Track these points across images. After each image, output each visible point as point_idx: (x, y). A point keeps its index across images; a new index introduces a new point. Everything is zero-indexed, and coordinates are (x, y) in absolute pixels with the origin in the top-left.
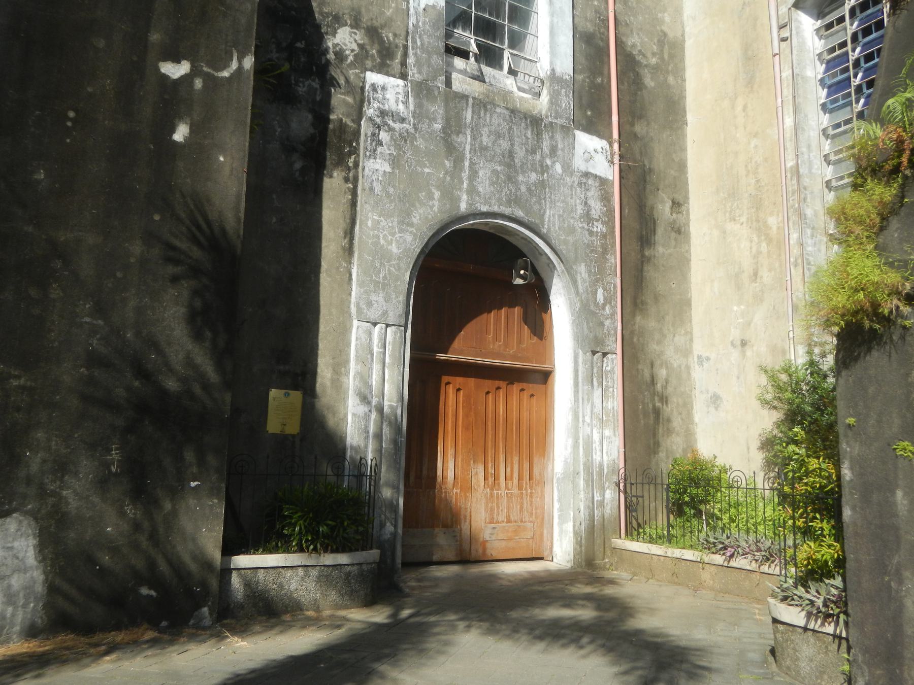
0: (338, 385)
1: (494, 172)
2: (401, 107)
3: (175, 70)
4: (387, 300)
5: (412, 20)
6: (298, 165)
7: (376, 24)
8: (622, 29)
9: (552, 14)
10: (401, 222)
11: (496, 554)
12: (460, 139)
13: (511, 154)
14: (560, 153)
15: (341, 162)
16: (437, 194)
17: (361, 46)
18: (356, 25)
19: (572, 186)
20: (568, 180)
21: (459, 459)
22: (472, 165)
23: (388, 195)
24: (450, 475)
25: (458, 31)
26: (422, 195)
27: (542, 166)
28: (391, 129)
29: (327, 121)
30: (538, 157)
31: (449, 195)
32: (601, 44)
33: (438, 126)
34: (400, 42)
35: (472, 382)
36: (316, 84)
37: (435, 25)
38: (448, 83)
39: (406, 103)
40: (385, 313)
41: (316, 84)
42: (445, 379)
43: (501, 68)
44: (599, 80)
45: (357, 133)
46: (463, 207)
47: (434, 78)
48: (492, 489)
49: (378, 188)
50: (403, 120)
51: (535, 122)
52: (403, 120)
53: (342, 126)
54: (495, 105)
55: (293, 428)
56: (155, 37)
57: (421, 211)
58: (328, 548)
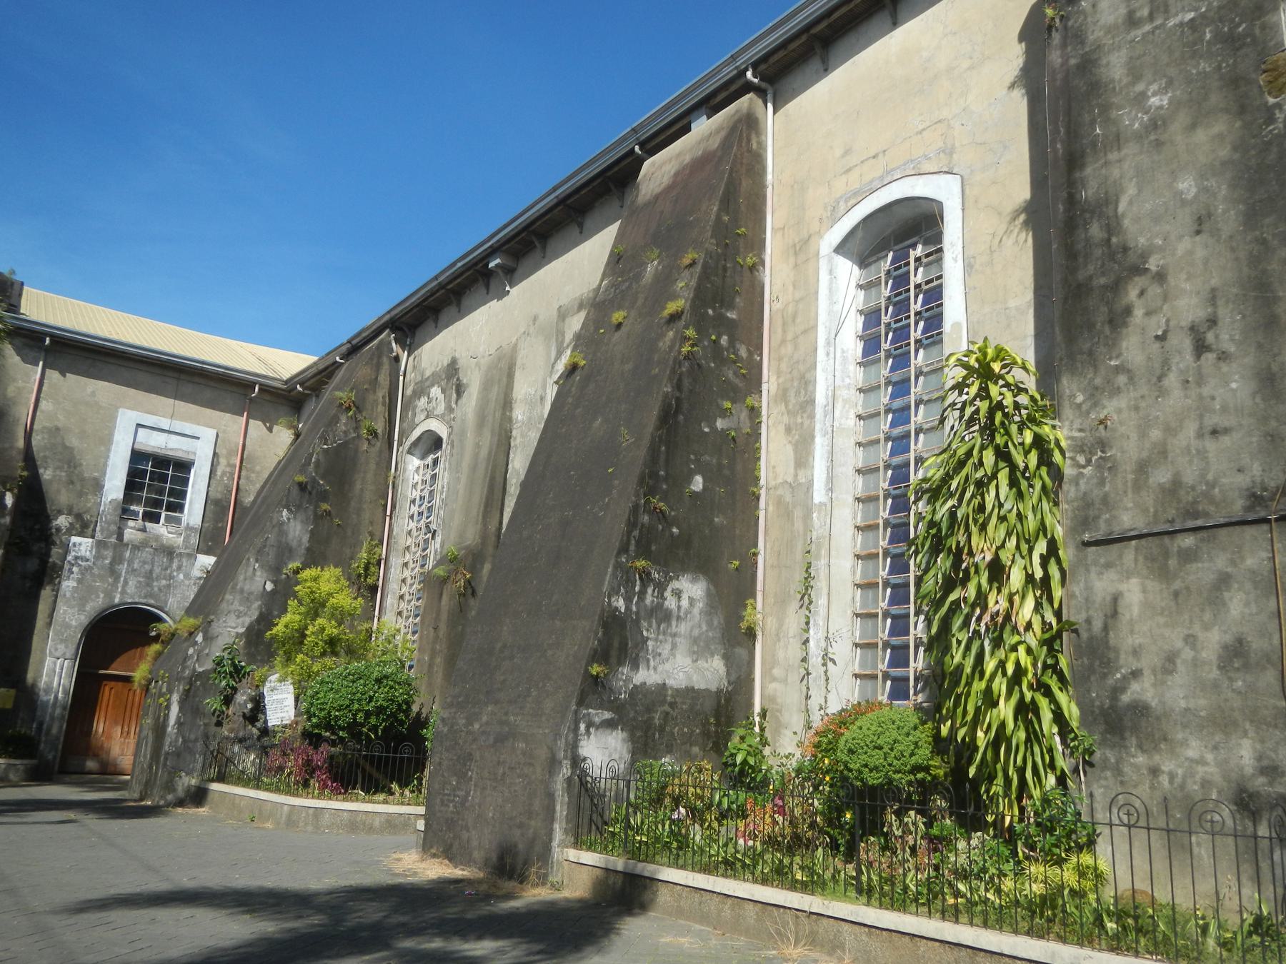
1: (139, 582)
4: (66, 647)
5: (102, 508)
6: (28, 585)
8: (241, 494)
9: (192, 493)
12: (121, 566)
13: (151, 571)
15: (51, 581)
16: (102, 595)
18: (69, 514)
20: (187, 582)
21: (107, 723)
24: (101, 730)
26: (93, 596)
28: (80, 565)
29: (48, 562)
31: (109, 594)
32: (225, 504)
33: (107, 562)
34: (94, 519)
35: (120, 684)
36: (43, 545)
37: (115, 510)
38: (120, 536)
39: (91, 551)
40: (64, 654)
42: (105, 683)
43: (158, 522)
45: (62, 568)
46: (117, 601)
47: (110, 537)
49: (68, 594)
50: (87, 560)
51: (169, 552)
52: (87, 560)
53: (54, 564)
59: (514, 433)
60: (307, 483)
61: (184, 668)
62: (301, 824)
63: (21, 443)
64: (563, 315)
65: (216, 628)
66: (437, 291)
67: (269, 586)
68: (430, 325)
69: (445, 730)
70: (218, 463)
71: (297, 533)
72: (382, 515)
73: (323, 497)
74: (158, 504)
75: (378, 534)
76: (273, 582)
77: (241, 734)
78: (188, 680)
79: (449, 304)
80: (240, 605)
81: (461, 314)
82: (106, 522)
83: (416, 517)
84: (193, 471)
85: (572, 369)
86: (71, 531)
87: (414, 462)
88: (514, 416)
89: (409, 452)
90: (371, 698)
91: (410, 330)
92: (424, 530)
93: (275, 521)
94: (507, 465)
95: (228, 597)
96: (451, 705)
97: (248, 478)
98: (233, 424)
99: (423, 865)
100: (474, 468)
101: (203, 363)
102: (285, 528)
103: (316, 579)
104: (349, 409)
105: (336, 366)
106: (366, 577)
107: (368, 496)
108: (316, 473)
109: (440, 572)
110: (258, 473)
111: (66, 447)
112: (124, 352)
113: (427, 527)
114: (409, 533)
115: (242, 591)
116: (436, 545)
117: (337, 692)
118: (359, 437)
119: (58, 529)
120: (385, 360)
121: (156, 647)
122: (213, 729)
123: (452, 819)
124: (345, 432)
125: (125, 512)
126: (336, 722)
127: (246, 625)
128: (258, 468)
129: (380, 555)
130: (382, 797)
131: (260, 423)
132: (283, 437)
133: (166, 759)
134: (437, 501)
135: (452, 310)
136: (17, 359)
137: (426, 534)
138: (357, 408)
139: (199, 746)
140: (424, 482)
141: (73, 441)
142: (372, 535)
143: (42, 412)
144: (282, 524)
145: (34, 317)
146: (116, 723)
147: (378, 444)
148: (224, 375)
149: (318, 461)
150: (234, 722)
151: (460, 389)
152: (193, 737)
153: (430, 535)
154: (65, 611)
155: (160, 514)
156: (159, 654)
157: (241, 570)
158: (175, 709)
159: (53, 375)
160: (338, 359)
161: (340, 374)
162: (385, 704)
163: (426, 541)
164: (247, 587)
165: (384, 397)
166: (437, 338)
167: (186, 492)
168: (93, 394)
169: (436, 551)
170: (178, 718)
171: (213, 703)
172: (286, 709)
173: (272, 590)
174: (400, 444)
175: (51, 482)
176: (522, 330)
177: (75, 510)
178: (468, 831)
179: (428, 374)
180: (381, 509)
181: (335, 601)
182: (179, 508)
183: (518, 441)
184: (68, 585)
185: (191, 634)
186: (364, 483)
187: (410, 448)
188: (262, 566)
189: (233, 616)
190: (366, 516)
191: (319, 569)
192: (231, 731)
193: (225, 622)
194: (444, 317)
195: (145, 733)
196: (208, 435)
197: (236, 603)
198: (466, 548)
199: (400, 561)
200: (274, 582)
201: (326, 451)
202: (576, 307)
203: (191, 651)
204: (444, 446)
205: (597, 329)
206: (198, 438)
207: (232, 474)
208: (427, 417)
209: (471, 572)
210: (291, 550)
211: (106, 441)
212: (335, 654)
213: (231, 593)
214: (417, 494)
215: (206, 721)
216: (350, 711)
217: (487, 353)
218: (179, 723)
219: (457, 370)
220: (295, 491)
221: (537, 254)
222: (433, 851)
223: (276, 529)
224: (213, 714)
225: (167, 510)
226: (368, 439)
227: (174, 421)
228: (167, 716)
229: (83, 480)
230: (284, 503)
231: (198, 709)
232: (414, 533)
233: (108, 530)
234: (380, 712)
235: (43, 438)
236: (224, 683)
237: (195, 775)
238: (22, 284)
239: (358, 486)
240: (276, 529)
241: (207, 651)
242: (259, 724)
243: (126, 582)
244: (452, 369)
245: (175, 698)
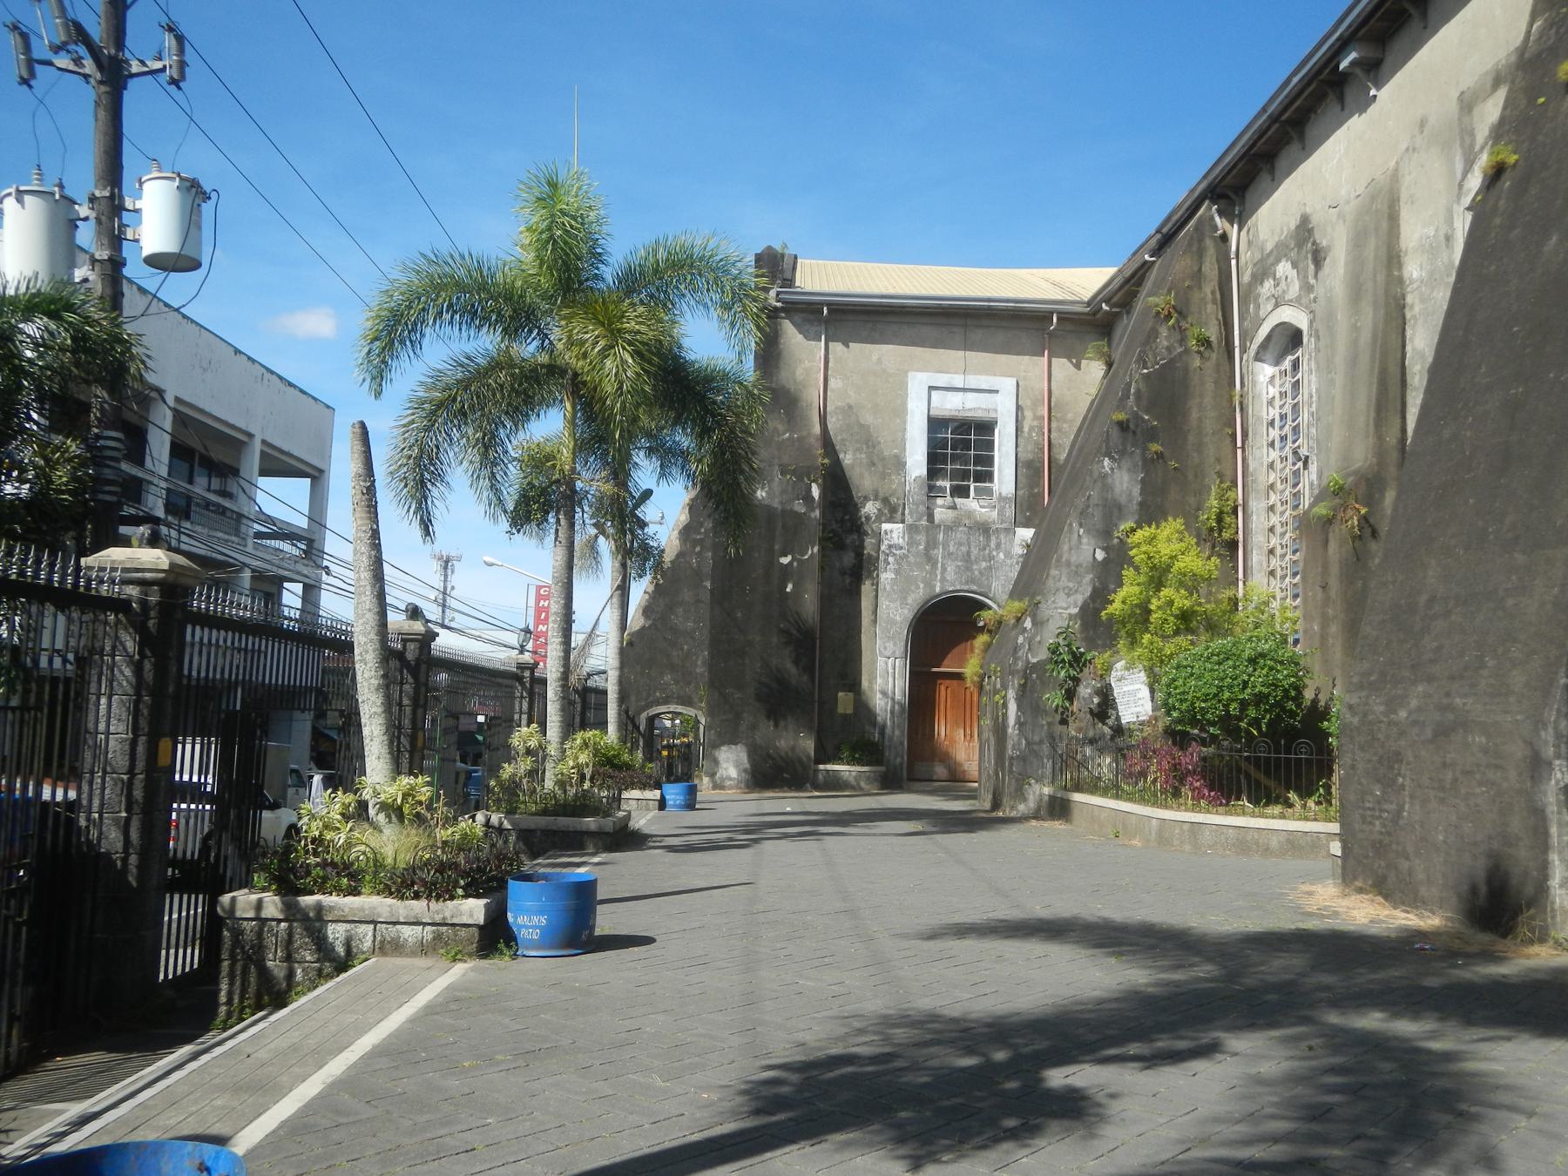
0: (871, 688)
1: (958, 567)
2: (901, 540)
3: (785, 560)
4: (895, 645)
5: (907, 488)
6: (848, 581)
7: (887, 495)
8: (1054, 450)
9: (1000, 458)
10: (902, 604)
11: (971, 779)
12: (936, 551)
13: (968, 553)
14: (1003, 546)
15: (870, 576)
16: (922, 586)
17: (879, 510)
18: (876, 499)
19: (1011, 565)
22: (943, 565)
23: (894, 590)
24: (943, 734)
25: (939, 483)
26: (913, 587)
27: (990, 557)
28: (895, 555)
29: (863, 555)
30: (987, 552)
32: (1038, 465)
34: (901, 502)
40: (894, 652)
41: (856, 537)
42: (939, 682)
43: (968, 497)
44: (1036, 491)
46: (938, 590)
47: (920, 520)
48: (969, 742)
49: (888, 588)
51: (984, 529)
54: (959, 525)
55: (850, 711)
56: (777, 547)
57: (913, 596)
58: (860, 762)
59: (1409, 299)
60: (1128, 420)
61: (1016, 659)
62: (1176, 842)
63: (817, 429)
64: (1467, 104)
65: (1045, 610)
66: (1269, 128)
67: (1100, 555)
68: (1264, 180)
69: (1356, 720)
70: (1024, 417)
71: (1125, 485)
72: (1230, 447)
73: (1152, 435)
74: (965, 475)
75: (1228, 473)
76: (1104, 549)
77: (1091, 734)
78: (1021, 674)
79: (1288, 143)
80: (1069, 580)
81: (1307, 151)
82: (914, 503)
83: (1277, 445)
84: (996, 431)
85: (1496, 174)
86: (880, 518)
87: (1266, 371)
88: (1406, 275)
89: (1258, 358)
90: (1245, 684)
91: (1236, 193)
92: (1291, 459)
93: (1096, 474)
94: (1404, 346)
95: (1054, 572)
96: (1361, 687)
97: (1059, 430)
98: (1033, 367)
99: (1345, 902)
100: (1353, 361)
101: (989, 300)
102: (1110, 480)
103: (1151, 540)
104: (1169, 316)
105: (1145, 267)
106: (1220, 531)
107: (1209, 426)
108: (1138, 407)
109: (1322, 510)
110: (1071, 421)
111: (862, 426)
112: (903, 307)
113: (1295, 453)
114: (1271, 466)
115: (1068, 564)
116: (1311, 476)
117: (1199, 678)
118: (1187, 351)
119: (868, 518)
120: (1209, 243)
121: (983, 639)
122: (1059, 729)
123: (1381, 842)
124: (1168, 349)
125: (932, 491)
126: (1203, 715)
127: (1080, 604)
128: (1070, 416)
129: (1236, 500)
130: (1277, 809)
131: (1065, 360)
132: (1094, 370)
133: (1011, 765)
134: (1305, 417)
135: (1294, 148)
136: (800, 337)
137: (1294, 464)
138: (1180, 313)
139: (1046, 748)
140: (1283, 395)
141: (868, 418)
142: (1220, 475)
143: (833, 391)
144: (1105, 476)
145: (809, 289)
146: (957, 724)
147: (1214, 356)
148: (1015, 310)
149: (1138, 391)
150: (1081, 721)
151: (1318, 257)
152: (1036, 738)
153: (1300, 464)
154: (888, 606)
155: (969, 486)
156: (988, 646)
157: (1064, 538)
158: (1012, 707)
159: (836, 347)
160: (1147, 257)
161: (1153, 275)
162: (1266, 690)
163: (1296, 474)
164: (1073, 559)
165: (1213, 293)
166: (1276, 195)
167: (993, 456)
168: (879, 361)
169: (1311, 484)
170: (1018, 718)
171: (1054, 698)
172: (1140, 702)
173: (1105, 559)
174: (1244, 350)
175: (853, 466)
176: (1404, 146)
177: (881, 495)
178: (1407, 858)
179: (1269, 246)
180: (1228, 440)
181: (1182, 565)
182: (986, 476)
183: (1417, 309)
184: (886, 577)
185: (1018, 619)
186: (1202, 410)
187: (1257, 353)
188: (1088, 532)
189: (1062, 595)
190: (1211, 451)
191: (1153, 526)
192: (1079, 730)
193: (1054, 602)
194: (1282, 163)
195: (985, 735)
196: (1007, 385)
197: (1063, 578)
198: (1355, 473)
199: (1264, 505)
200: (1104, 549)
201: (1147, 376)
202: (1488, 86)
203: (1020, 640)
204: (1305, 340)
205: (1532, 101)
206: (997, 392)
207: (1041, 428)
208: (1277, 306)
209: (1367, 505)
210: (1120, 508)
211: (901, 412)
212: (1190, 631)
213: (1056, 567)
214: (1274, 413)
215: (1050, 720)
216: (1220, 701)
217: (1353, 195)
218: (1020, 724)
219: (1310, 231)
220: (1115, 433)
221: (1415, 25)
222: (1359, 884)
223: (1099, 484)
224: (1056, 711)
225: (974, 482)
226: (1199, 352)
227: (968, 377)
228: (1005, 716)
229: (883, 459)
230: (1104, 450)
231: (1038, 706)
232: (1278, 466)
233: (918, 512)
234: (1261, 701)
235: (838, 419)
236: (1063, 673)
237: (1046, 781)
238: (796, 257)
239: (1195, 414)
240: (1099, 484)
241: (1038, 638)
242: (1110, 722)
243: (944, 569)
244: (1304, 231)
245: (1011, 694)
